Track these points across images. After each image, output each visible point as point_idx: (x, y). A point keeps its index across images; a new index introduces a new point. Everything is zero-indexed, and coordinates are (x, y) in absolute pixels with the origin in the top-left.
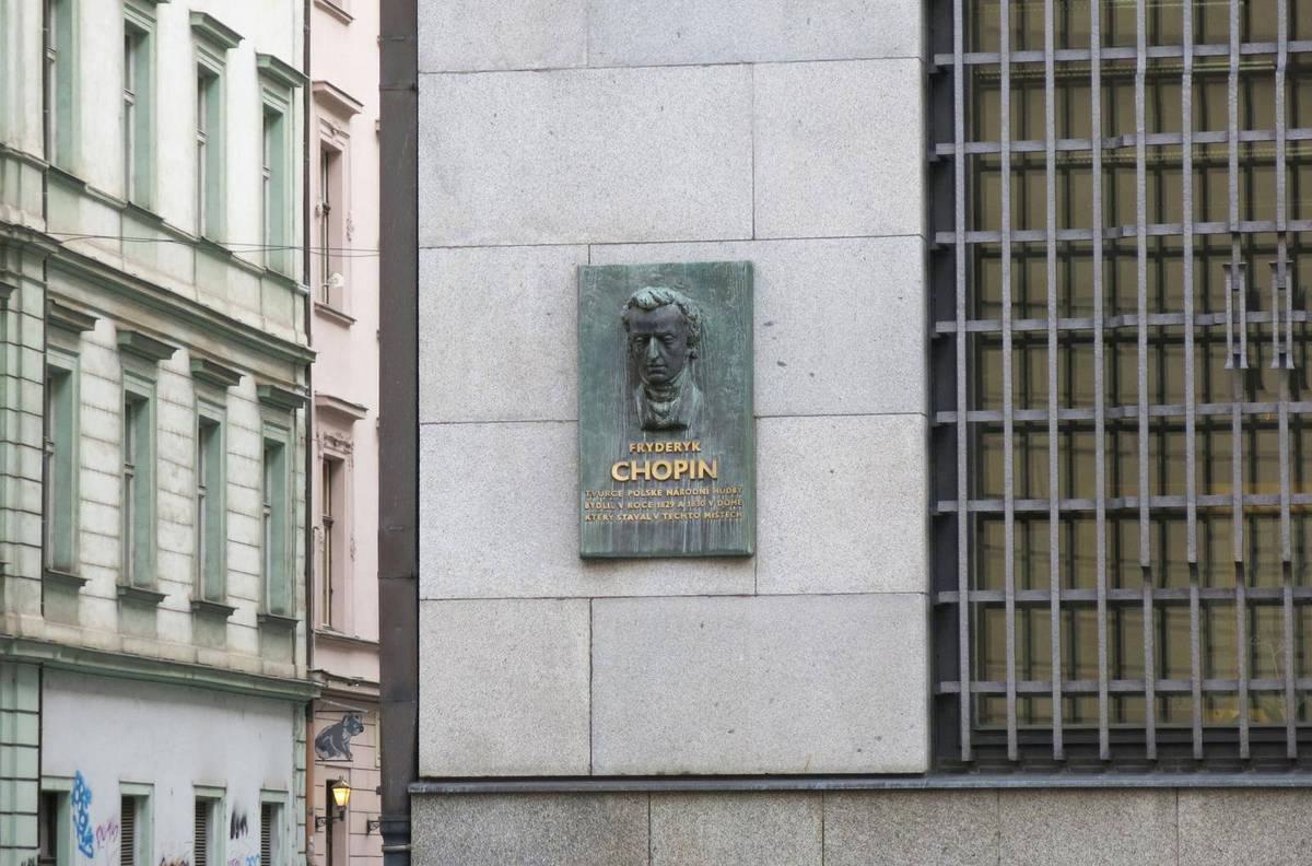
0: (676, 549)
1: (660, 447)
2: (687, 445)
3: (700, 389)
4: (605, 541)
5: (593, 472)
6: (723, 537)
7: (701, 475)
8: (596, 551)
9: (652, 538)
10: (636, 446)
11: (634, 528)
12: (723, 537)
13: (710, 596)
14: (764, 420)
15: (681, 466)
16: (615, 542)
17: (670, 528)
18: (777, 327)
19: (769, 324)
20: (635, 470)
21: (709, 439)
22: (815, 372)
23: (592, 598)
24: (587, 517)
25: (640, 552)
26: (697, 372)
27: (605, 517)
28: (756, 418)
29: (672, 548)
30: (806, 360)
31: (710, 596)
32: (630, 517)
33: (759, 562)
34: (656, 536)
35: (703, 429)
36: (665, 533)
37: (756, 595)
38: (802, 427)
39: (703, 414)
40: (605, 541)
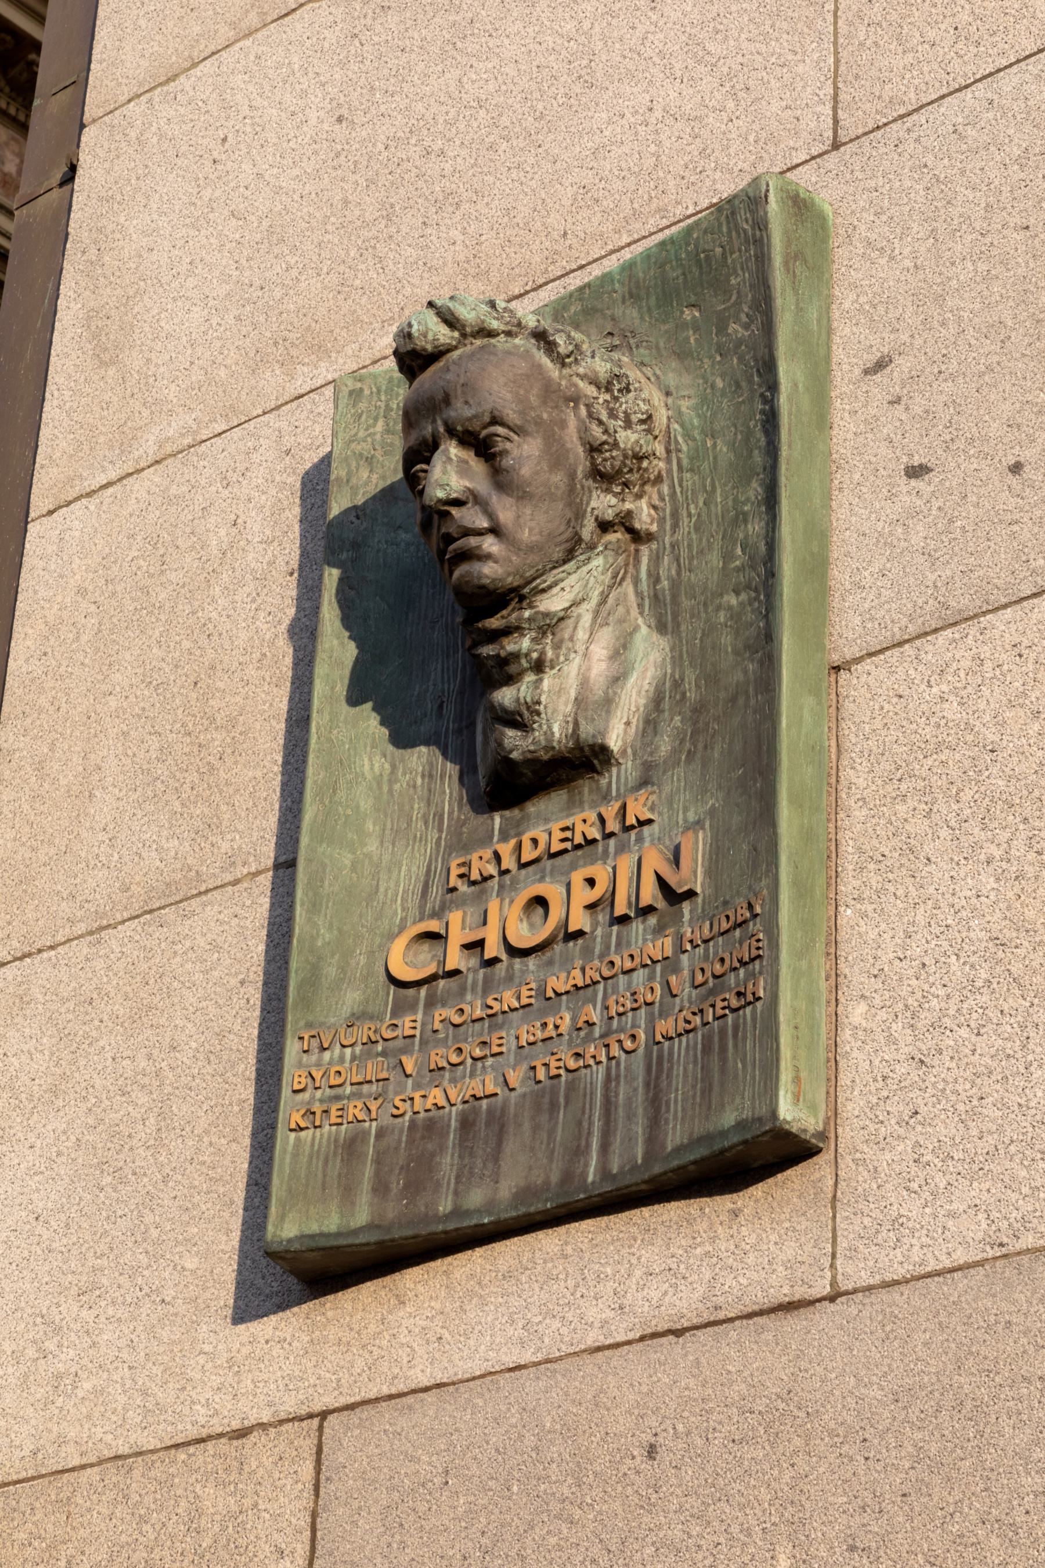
0: (567, 1177)
1: (535, 841)
2: (610, 812)
3: (661, 628)
4: (348, 1192)
5: (331, 971)
6: (707, 1091)
7: (649, 893)
8: (314, 1228)
9: (496, 1157)
10: (468, 864)
11: (444, 1133)
12: (707, 1091)
13: (678, 1333)
14: (867, 665)
15: (591, 882)
16: (380, 1188)
17: (554, 1106)
18: (902, 366)
19: (880, 365)
20: (457, 936)
21: (680, 771)
22: (1027, 455)
23: (324, 1415)
24: (297, 1118)
25: (457, 1212)
26: (655, 579)
27: (355, 1110)
28: (837, 669)
29: (555, 1178)
30: (995, 429)
31: (678, 1333)
32: (436, 1096)
33: (846, 1162)
34: (510, 1146)
35: (664, 745)
36: (536, 1128)
37: (832, 1299)
38: (985, 651)
39: (666, 705)
40: (348, 1192)
